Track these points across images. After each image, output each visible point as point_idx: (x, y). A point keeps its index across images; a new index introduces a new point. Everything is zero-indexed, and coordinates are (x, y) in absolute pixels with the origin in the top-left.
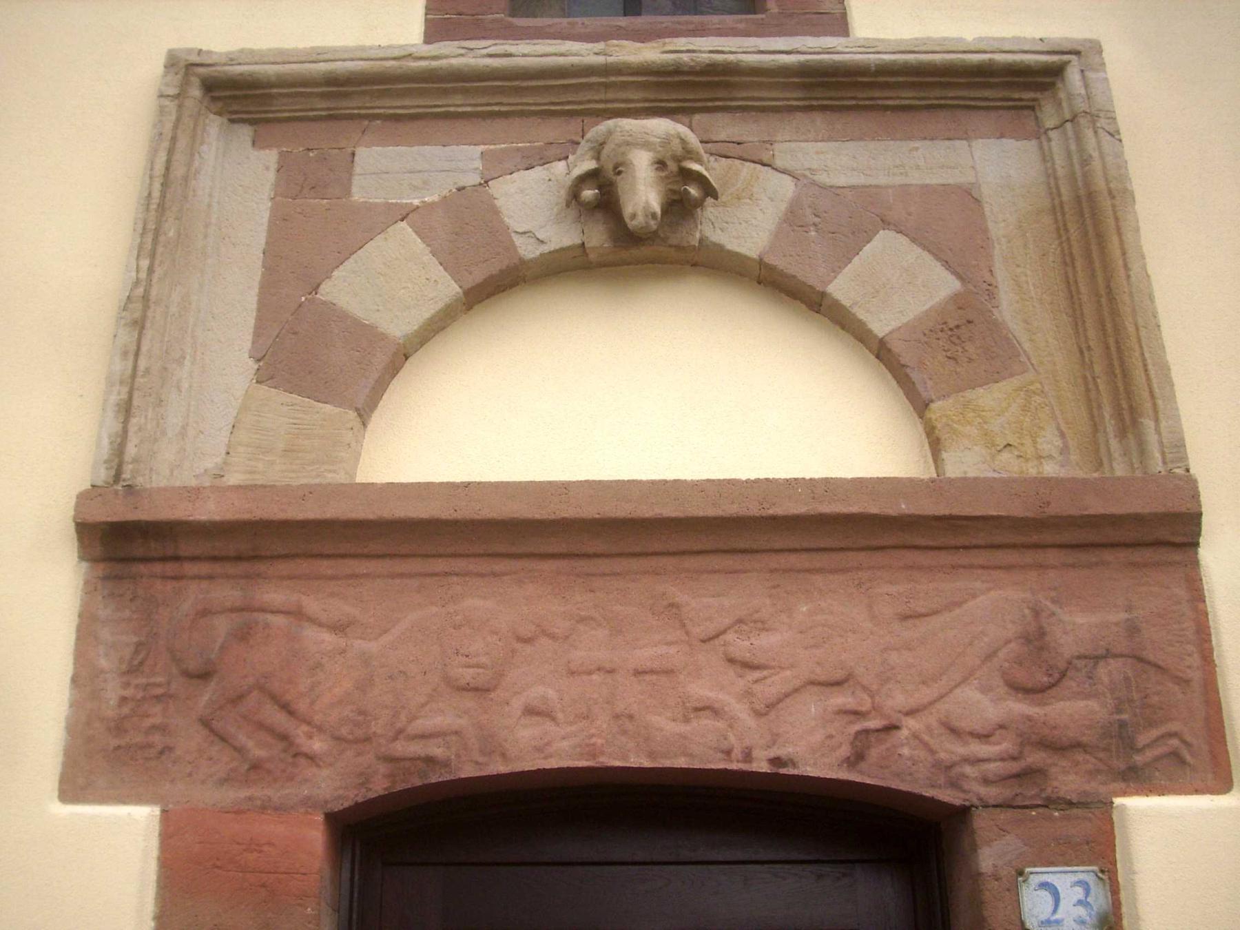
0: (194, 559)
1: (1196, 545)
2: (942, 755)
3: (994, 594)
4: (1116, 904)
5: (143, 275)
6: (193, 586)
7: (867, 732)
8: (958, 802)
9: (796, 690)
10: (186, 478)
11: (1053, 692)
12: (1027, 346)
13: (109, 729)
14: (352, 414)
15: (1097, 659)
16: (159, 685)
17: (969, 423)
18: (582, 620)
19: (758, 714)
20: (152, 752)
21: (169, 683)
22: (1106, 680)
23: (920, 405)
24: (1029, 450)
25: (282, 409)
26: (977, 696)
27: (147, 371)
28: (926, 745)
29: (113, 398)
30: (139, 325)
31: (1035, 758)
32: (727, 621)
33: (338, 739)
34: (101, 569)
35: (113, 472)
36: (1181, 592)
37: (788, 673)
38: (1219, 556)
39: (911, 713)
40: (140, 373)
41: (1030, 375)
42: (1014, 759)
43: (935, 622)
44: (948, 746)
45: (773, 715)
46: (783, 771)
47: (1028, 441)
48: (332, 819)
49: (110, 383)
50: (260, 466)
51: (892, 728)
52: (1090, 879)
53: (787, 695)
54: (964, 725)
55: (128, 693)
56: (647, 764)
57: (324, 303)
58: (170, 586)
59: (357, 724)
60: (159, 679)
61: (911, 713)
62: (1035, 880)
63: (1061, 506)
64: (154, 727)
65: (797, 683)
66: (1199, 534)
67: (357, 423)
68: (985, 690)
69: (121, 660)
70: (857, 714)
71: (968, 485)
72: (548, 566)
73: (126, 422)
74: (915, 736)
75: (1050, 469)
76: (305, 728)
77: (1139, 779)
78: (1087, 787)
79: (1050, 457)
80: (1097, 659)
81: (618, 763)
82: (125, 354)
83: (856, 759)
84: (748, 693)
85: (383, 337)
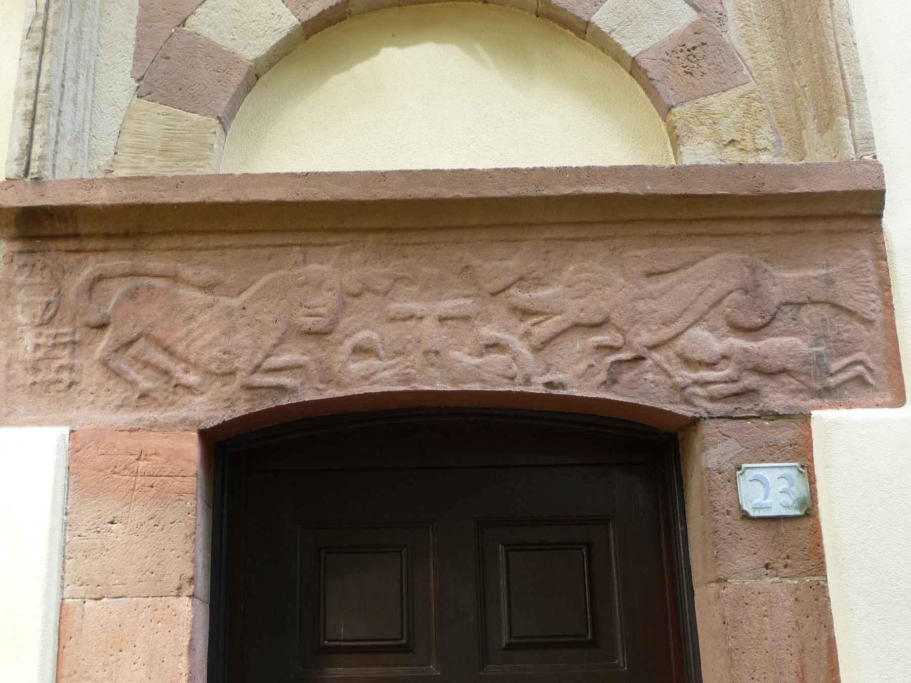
0: (91, 236)
1: (880, 216)
2: (678, 379)
3: (720, 257)
4: (813, 492)
5: (41, 10)
6: (92, 257)
7: (620, 362)
8: (690, 414)
9: (565, 331)
10: (82, 172)
11: (765, 330)
12: (749, 63)
13: (26, 369)
14: (215, 122)
15: (800, 304)
16: (66, 334)
17: (702, 124)
18: (397, 279)
19: (536, 350)
20: (62, 386)
21: (74, 333)
22: (807, 321)
23: (665, 110)
24: (750, 146)
25: (156, 118)
26: (706, 334)
27: (48, 88)
28: (665, 371)
29: (21, 109)
30: (40, 50)
31: (751, 381)
32: (512, 279)
33: (208, 373)
34: (17, 246)
35: (23, 168)
36: (866, 253)
37: (558, 318)
38: (895, 222)
39: (654, 347)
40: (42, 89)
41: (752, 85)
42: (734, 381)
43: (673, 278)
44: (684, 372)
45: (547, 350)
46: (555, 392)
47: (748, 137)
48: (206, 435)
49: (18, 97)
50: (143, 163)
51: (639, 359)
52: (793, 473)
53: (558, 335)
54: (696, 356)
55: (41, 340)
56: (449, 388)
57: (189, 34)
58: (72, 258)
59: (224, 362)
60: (65, 330)
61: (654, 347)
62: (749, 474)
63: (773, 186)
64: (61, 368)
65: (565, 325)
66: (882, 208)
67: (219, 129)
68: (712, 329)
69: (34, 316)
70: (613, 349)
71: (699, 170)
72: (371, 239)
73: (32, 128)
74: (657, 365)
75: (765, 158)
76: (183, 365)
77: (829, 395)
78: (791, 403)
79: (765, 149)
80: (800, 304)
81: (427, 388)
82: (29, 73)
83: (611, 381)
84: (527, 334)
85: (238, 61)
